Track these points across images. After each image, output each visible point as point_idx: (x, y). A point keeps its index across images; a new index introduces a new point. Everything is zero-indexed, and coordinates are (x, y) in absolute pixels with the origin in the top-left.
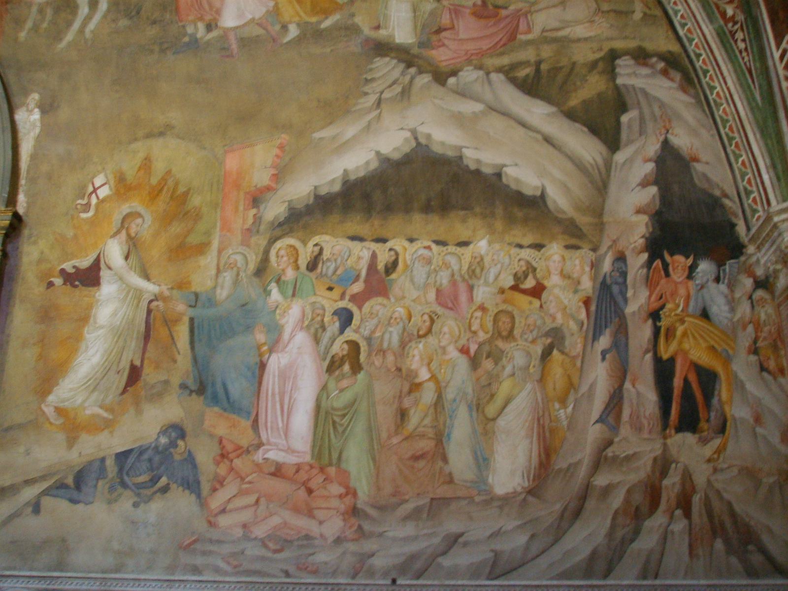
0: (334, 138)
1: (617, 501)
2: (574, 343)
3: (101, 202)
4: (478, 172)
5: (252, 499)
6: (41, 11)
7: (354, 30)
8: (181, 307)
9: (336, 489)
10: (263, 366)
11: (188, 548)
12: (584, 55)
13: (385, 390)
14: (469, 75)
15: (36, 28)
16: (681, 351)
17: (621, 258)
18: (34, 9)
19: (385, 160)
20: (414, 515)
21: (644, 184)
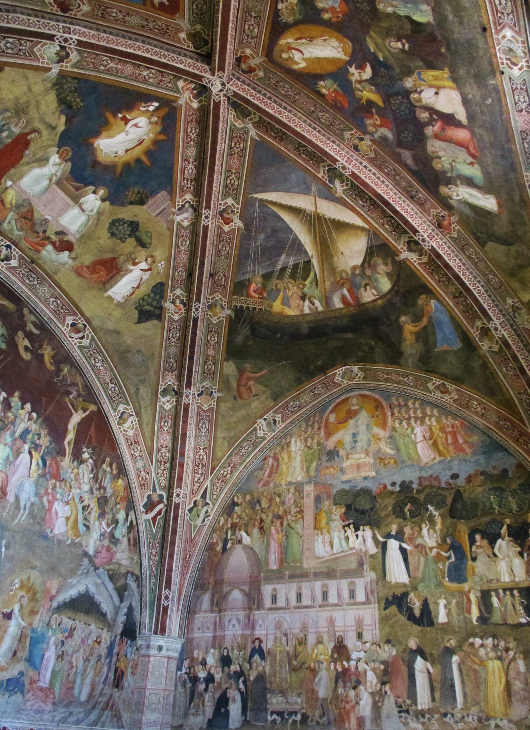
0: (71, 583)
1: (101, 706)
2: (103, 659)
3: (16, 589)
4: (96, 603)
5: (34, 697)
6: (11, 506)
7: (81, 545)
8: (29, 632)
9: (52, 696)
10: (44, 655)
11: (18, 712)
12: (123, 571)
13: (66, 667)
14: (101, 570)
15: (8, 513)
16: (120, 666)
17: (116, 637)
18: (9, 504)
19: (80, 594)
20: (65, 706)
21: (124, 615)
